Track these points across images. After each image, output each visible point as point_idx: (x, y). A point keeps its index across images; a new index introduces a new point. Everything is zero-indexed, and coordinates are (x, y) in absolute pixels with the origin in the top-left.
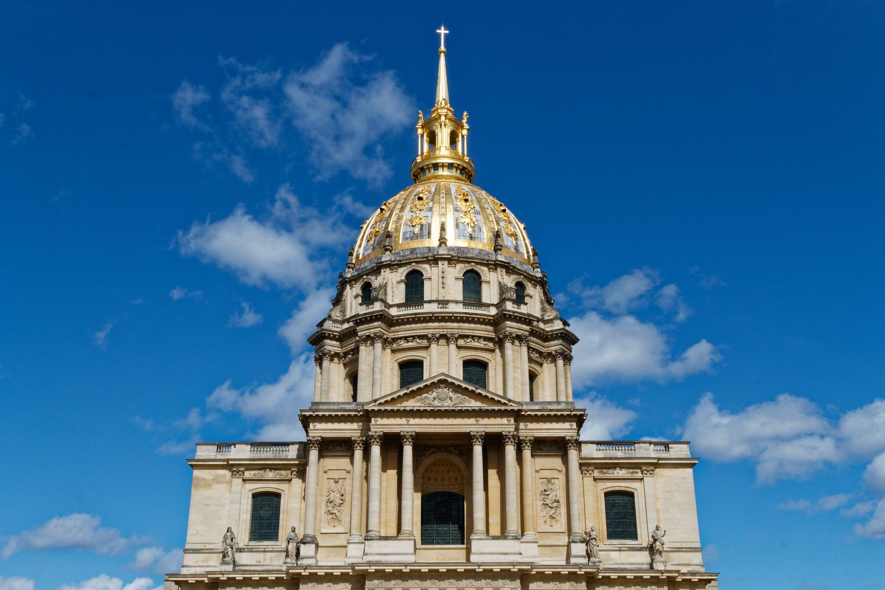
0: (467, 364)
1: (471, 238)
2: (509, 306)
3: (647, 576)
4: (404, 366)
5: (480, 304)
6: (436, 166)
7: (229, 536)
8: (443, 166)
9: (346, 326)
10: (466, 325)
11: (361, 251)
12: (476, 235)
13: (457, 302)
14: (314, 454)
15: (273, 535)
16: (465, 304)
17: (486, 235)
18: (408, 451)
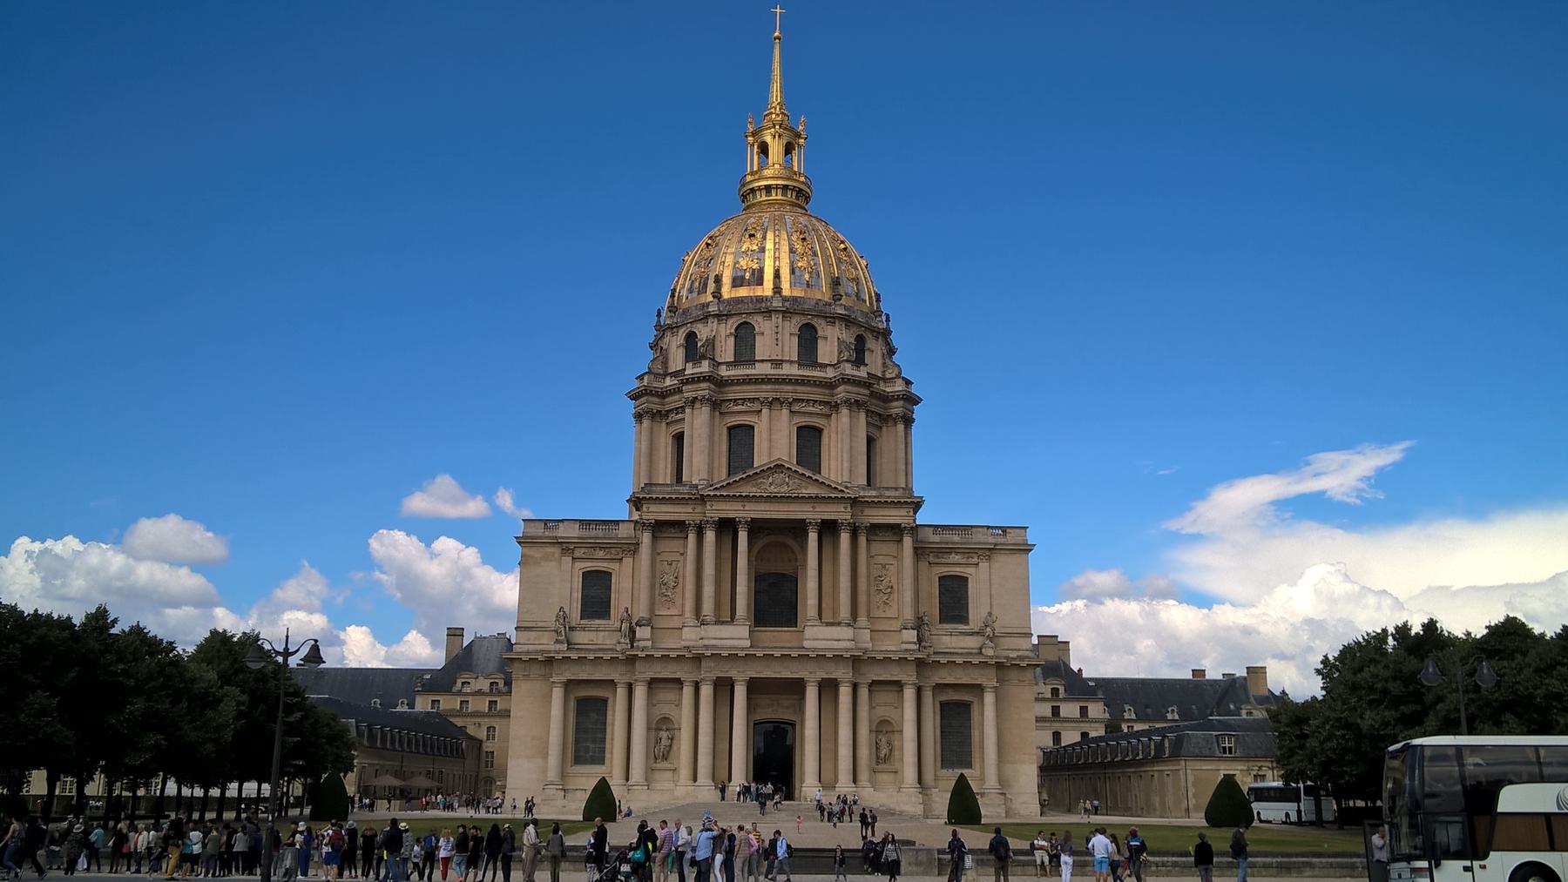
3: (976, 661)
4: (730, 429)
6: (768, 189)
7: (563, 616)
8: (777, 187)
9: (668, 382)
10: (800, 388)
11: (684, 293)
14: (646, 538)
17: (824, 283)
18: (743, 536)
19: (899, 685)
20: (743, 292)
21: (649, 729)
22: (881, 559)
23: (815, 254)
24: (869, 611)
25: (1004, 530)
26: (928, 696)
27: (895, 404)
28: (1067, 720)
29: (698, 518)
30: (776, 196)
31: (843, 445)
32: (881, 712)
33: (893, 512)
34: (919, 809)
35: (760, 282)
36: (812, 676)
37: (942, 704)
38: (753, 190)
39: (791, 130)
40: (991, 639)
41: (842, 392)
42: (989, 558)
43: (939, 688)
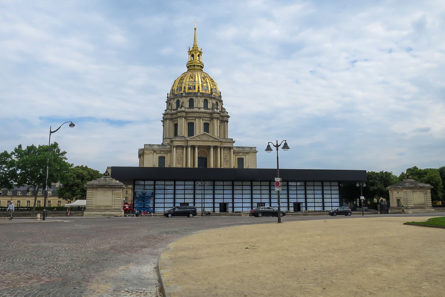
2: (215, 110)
6: (194, 65)
9: (173, 111)
18: (197, 149)
22: (226, 154)
23: (207, 82)
25: (251, 148)
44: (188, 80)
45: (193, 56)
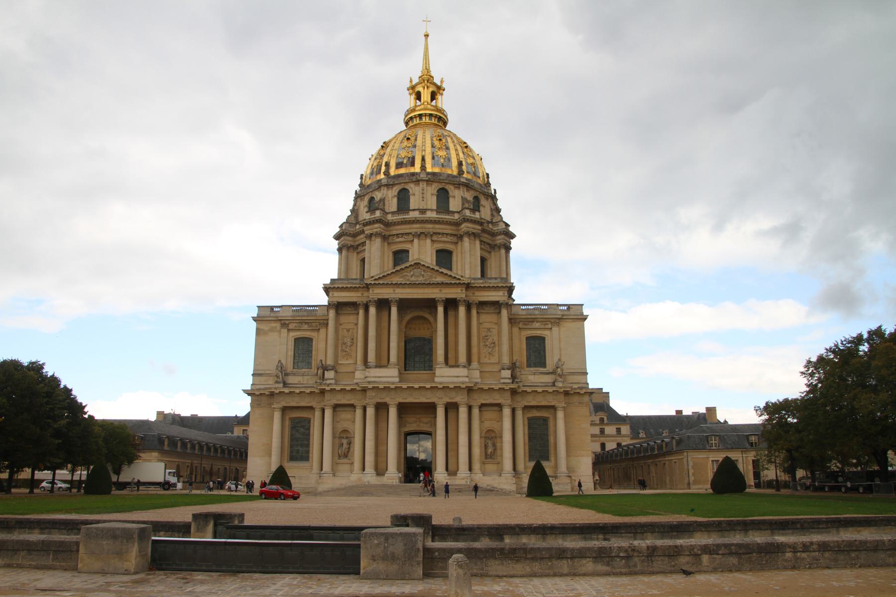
0: (439, 252)
1: (443, 166)
3: (551, 390)
5: (448, 211)
6: (420, 116)
7: (281, 367)
8: (426, 115)
9: (358, 227)
10: (437, 226)
12: (445, 164)
13: (432, 210)
15: (309, 365)
16: (438, 212)
18: (394, 310)
19: (499, 406)
20: (402, 171)
21: (334, 437)
22: (487, 325)
24: (479, 358)
25: (569, 307)
26: (519, 413)
27: (499, 237)
28: (608, 436)
29: (365, 300)
30: (426, 120)
31: (467, 259)
32: (488, 425)
33: (494, 293)
34: (513, 488)
35: (413, 164)
36: (441, 401)
37: (529, 419)
38: (411, 118)
39: (435, 84)
40: (560, 376)
41: (465, 227)
42: (558, 324)
43: (526, 408)
44: (397, 146)
45: (418, 96)
